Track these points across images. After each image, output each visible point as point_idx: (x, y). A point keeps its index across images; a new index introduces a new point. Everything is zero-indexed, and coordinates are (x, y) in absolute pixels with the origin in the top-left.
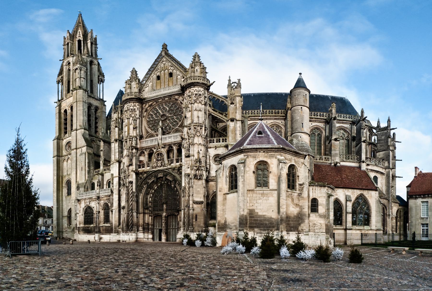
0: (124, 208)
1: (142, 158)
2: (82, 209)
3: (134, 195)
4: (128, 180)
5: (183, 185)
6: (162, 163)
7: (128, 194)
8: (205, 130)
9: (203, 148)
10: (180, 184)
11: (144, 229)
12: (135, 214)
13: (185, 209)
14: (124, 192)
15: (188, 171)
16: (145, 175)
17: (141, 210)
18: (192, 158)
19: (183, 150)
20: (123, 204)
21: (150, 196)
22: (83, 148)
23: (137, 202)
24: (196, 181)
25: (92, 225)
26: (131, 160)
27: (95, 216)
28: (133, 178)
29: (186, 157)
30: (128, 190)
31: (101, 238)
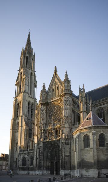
1: (46, 135)
2: (21, 158)
5: (61, 148)
8: (70, 119)
9: (69, 129)
10: (60, 148)
11: (46, 168)
12: (42, 161)
14: (38, 151)
15: (63, 141)
16: (47, 143)
17: (45, 160)
20: (38, 157)
23: (43, 156)
24: (66, 145)
25: (25, 167)
27: (27, 162)
28: (42, 144)
31: (29, 173)
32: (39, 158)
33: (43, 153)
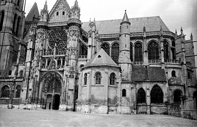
0: (30, 90)
3: (37, 83)
4: (34, 75)
6: (54, 67)
7: (34, 82)
8: (77, 51)
13: (64, 93)
18: (69, 67)
19: (65, 62)
21: (46, 84)
22: (7, 47)
23: (39, 87)
26: (38, 63)
28: (38, 73)
29: (66, 66)
30: (34, 80)
32: (32, 89)
33: (39, 84)
